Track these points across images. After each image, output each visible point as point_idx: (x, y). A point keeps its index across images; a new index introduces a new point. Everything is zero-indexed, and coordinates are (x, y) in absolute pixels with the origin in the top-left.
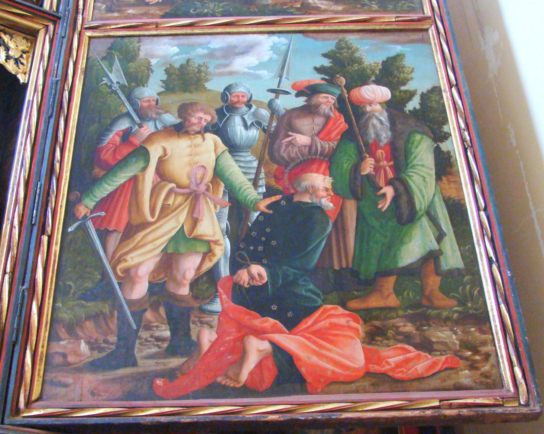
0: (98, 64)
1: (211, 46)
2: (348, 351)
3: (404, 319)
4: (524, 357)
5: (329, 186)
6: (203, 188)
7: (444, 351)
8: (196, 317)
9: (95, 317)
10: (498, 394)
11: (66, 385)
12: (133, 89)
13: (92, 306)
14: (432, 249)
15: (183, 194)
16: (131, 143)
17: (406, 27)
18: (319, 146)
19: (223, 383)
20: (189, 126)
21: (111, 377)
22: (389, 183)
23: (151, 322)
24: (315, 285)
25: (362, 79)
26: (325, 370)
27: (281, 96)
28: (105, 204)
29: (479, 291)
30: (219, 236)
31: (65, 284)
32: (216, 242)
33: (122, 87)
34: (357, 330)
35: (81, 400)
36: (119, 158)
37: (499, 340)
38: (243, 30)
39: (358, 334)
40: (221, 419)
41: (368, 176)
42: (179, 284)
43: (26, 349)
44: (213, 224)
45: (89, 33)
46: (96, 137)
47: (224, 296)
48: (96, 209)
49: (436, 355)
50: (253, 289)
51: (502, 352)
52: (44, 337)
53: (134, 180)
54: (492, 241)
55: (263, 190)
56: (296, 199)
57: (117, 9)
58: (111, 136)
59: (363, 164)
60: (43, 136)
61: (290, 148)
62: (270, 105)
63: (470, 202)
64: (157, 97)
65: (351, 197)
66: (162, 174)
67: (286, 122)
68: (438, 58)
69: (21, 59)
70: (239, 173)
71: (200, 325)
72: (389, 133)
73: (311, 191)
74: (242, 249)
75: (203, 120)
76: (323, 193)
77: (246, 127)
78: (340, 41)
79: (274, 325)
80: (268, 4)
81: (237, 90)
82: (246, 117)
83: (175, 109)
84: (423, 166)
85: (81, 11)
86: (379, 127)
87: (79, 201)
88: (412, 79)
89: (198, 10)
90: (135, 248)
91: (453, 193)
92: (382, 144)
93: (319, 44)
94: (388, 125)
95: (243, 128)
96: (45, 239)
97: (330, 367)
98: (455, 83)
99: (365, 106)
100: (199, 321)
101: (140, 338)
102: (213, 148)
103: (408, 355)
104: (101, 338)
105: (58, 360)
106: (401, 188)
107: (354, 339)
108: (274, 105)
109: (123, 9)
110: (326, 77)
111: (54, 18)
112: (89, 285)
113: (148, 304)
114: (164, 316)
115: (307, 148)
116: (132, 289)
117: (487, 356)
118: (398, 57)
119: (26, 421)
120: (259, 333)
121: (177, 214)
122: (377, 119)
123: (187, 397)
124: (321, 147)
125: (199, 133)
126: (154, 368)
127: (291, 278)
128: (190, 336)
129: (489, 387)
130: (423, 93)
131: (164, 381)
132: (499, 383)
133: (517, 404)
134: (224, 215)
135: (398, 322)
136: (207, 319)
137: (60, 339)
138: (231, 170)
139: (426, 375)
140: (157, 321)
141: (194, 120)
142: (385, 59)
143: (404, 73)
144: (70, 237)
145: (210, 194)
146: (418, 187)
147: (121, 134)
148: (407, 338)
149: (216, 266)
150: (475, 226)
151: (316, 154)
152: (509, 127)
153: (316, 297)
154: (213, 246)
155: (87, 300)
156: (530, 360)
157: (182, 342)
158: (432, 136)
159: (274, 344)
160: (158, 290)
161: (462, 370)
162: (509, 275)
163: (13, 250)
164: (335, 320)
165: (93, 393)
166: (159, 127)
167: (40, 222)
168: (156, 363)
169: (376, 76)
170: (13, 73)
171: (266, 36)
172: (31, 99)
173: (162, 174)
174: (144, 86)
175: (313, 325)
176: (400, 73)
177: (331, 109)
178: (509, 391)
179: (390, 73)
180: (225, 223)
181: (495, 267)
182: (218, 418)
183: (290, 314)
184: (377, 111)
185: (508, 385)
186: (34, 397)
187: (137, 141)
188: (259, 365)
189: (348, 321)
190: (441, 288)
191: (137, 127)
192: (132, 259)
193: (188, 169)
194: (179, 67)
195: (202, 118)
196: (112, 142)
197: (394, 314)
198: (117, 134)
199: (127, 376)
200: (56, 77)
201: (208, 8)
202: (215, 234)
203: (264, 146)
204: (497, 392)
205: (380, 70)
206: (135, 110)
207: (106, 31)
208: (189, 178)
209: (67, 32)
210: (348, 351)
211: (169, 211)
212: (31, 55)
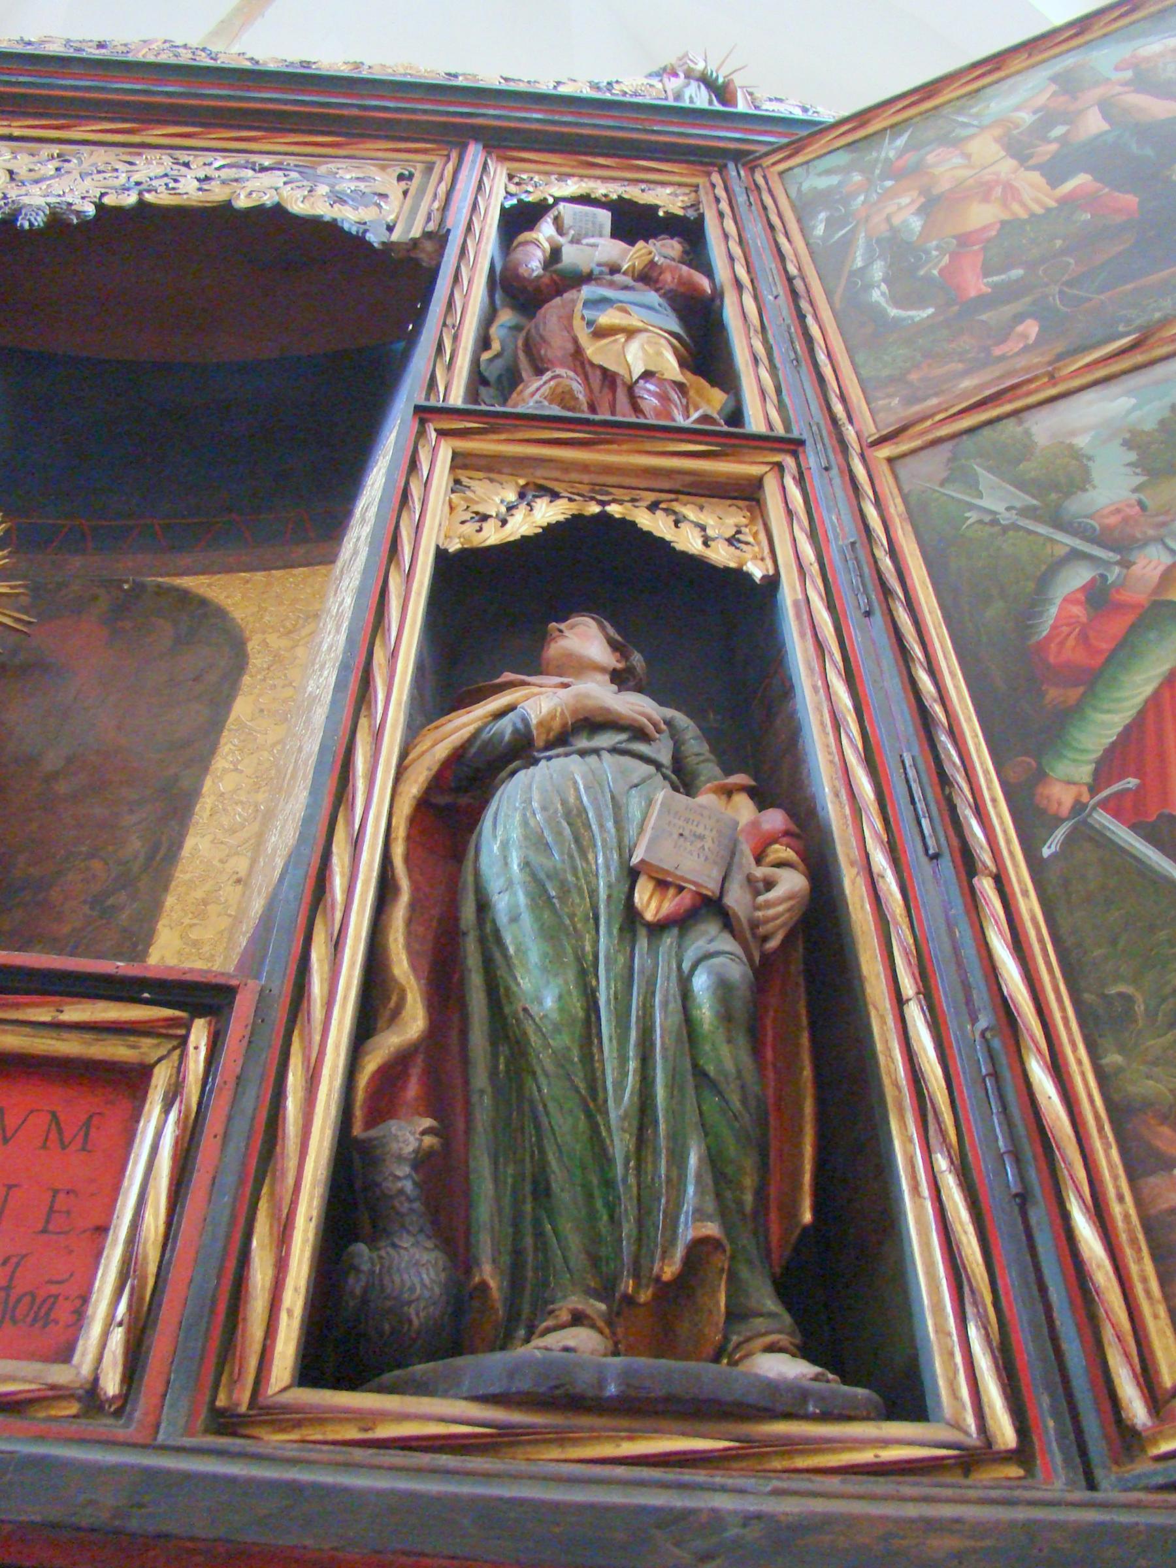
0: (936, 495)
16: (1120, 608)
31: (1104, 996)
43: (1066, 1217)
45: (885, 451)
58: (1053, 610)
64: (1136, 496)
87: (1040, 776)
96: (986, 885)
170: (733, 565)
172: (800, 596)
174: (1084, 490)
194: (1156, 427)
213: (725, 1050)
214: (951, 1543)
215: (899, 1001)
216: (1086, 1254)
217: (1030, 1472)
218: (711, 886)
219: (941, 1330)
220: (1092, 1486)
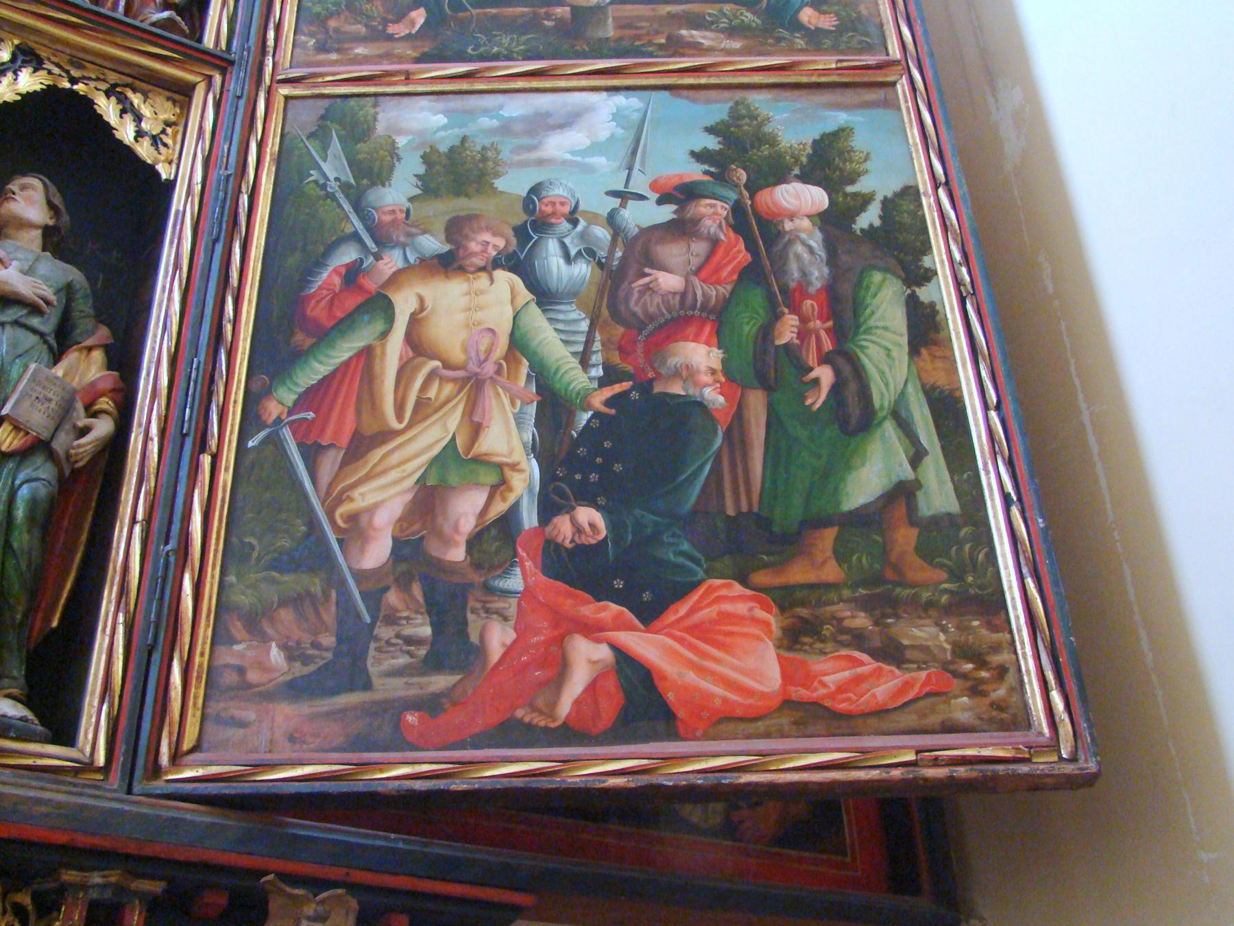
0: (301, 145)
1: (506, 113)
2: (750, 662)
3: (853, 605)
4: (1068, 673)
5: (717, 365)
6: (490, 368)
7: (925, 663)
8: (477, 600)
9: (296, 601)
10: (1021, 740)
11: (243, 724)
12: (365, 191)
13: (291, 582)
14: (903, 478)
15: (454, 380)
16: (361, 288)
17: (857, 79)
18: (699, 293)
19: (527, 719)
20: (464, 258)
21: (325, 708)
22: (824, 359)
23: (399, 611)
24: (693, 544)
25: (776, 172)
26: (710, 696)
27: (631, 204)
28: (313, 397)
29: (986, 555)
30: (519, 455)
31: (241, 542)
32: (514, 467)
33: (345, 187)
34: (767, 624)
35: (270, 751)
36: (340, 314)
37: (1022, 643)
38: (562, 84)
39: (769, 632)
40: (522, 785)
41: (787, 347)
42: (447, 542)
43: (171, 660)
44: (509, 433)
45: (285, 91)
46: (297, 276)
47: (528, 564)
48: (298, 406)
49: (911, 670)
50: (583, 553)
51: (1028, 664)
52: (205, 637)
53: (367, 355)
54: (1010, 464)
55: (598, 372)
56: (658, 388)
57: (336, 46)
58: (325, 275)
59: (778, 325)
60: (202, 274)
61: (647, 297)
62: (611, 220)
63: (970, 394)
64: (408, 204)
65: (756, 384)
66: (417, 344)
67: (640, 250)
68: (914, 134)
69: (162, 136)
70: (555, 341)
71: (485, 615)
72: (826, 270)
73: (684, 374)
74: (561, 479)
75: (490, 247)
76: (707, 379)
77: (568, 259)
78: (737, 103)
79: (619, 616)
80: (607, 39)
81: (551, 193)
82: (567, 241)
83: (440, 226)
84: (885, 328)
85: (271, 50)
86: (808, 257)
87: (268, 392)
88: (866, 172)
89: (482, 49)
90: (368, 478)
91: (940, 379)
92: (812, 290)
93: (699, 109)
94: (823, 254)
95: (562, 261)
96: (206, 460)
97: (718, 690)
98: (943, 179)
99: (782, 222)
100: (483, 607)
101: (377, 639)
102: (508, 296)
103: (859, 670)
104: (307, 639)
105: (230, 678)
106: (847, 370)
107: (762, 640)
108: (618, 219)
109: (347, 46)
110: (712, 169)
111: (222, 62)
112: (285, 543)
113: (392, 577)
114: (420, 598)
115: (678, 297)
116: (362, 550)
117: (1002, 671)
118: (842, 133)
119: (171, 788)
120: (592, 630)
121: (445, 415)
122: (804, 243)
123: (462, 745)
124: (704, 294)
125: (482, 269)
126: (401, 693)
127: (649, 531)
128: (467, 635)
129: (1005, 726)
130: (885, 198)
131: (420, 718)
132: (1022, 721)
133: (1055, 758)
134: (527, 417)
135: (842, 610)
136: (499, 604)
137: (232, 641)
138: (542, 337)
139: (891, 705)
140: (408, 608)
141: (474, 246)
142: (817, 137)
143: (851, 162)
144: (251, 456)
145: (503, 379)
146: (877, 367)
147: (343, 271)
148: (858, 639)
149: (514, 509)
150: (979, 437)
151: (693, 307)
152: (1041, 258)
153: (693, 566)
154: (508, 473)
155: (281, 571)
156: (1079, 677)
157: (452, 647)
158: (903, 275)
159: (617, 650)
160: (408, 551)
161: (956, 697)
162: (1042, 525)
163: (148, 480)
164: (727, 607)
165: (292, 739)
166: (412, 258)
167: (197, 429)
168: (406, 683)
169: (802, 167)
170: (149, 162)
171: (604, 95)
173: (417, 344)
174: (383, 185)
175: (688, 615)
176: (845, 161)
177: (720, 226)
178: (1041, 734)
179: (827, 162)
180: (530, 432)
181: (1015, 511)
182: (518, 783)
183: (647, 596)
184: (804, 231)
185: (1040, 724)
186: (187, 745)
187: (372, 284)
188: (592, 688)
189: (751, 609)
190: (918, 549)
191: (371, 259)
192: (363, 497)
193: (463, 335)
195: (489, 242)
196: (327, 285)
197: (833, 596)
198: (335, 271)
199: (354, 708)
200: (226, 169)
201: (500, 45)
202: (511, 452)
203: (601, 293)
204: (1019, 737)
205: (809, 156)
206: (368, 229)
207: (316, 85)
208: (465, 350)
209: (246, 87)
210: (750, 662)
211: (430, 410)
212: (181, 129)
213: (26, 537)
214: (43, 809)
215: (133, 521)
216: (172, 680)
217: (106, 778)
218: (45, 435)
219: (91, 705)
220: (129, 792)
